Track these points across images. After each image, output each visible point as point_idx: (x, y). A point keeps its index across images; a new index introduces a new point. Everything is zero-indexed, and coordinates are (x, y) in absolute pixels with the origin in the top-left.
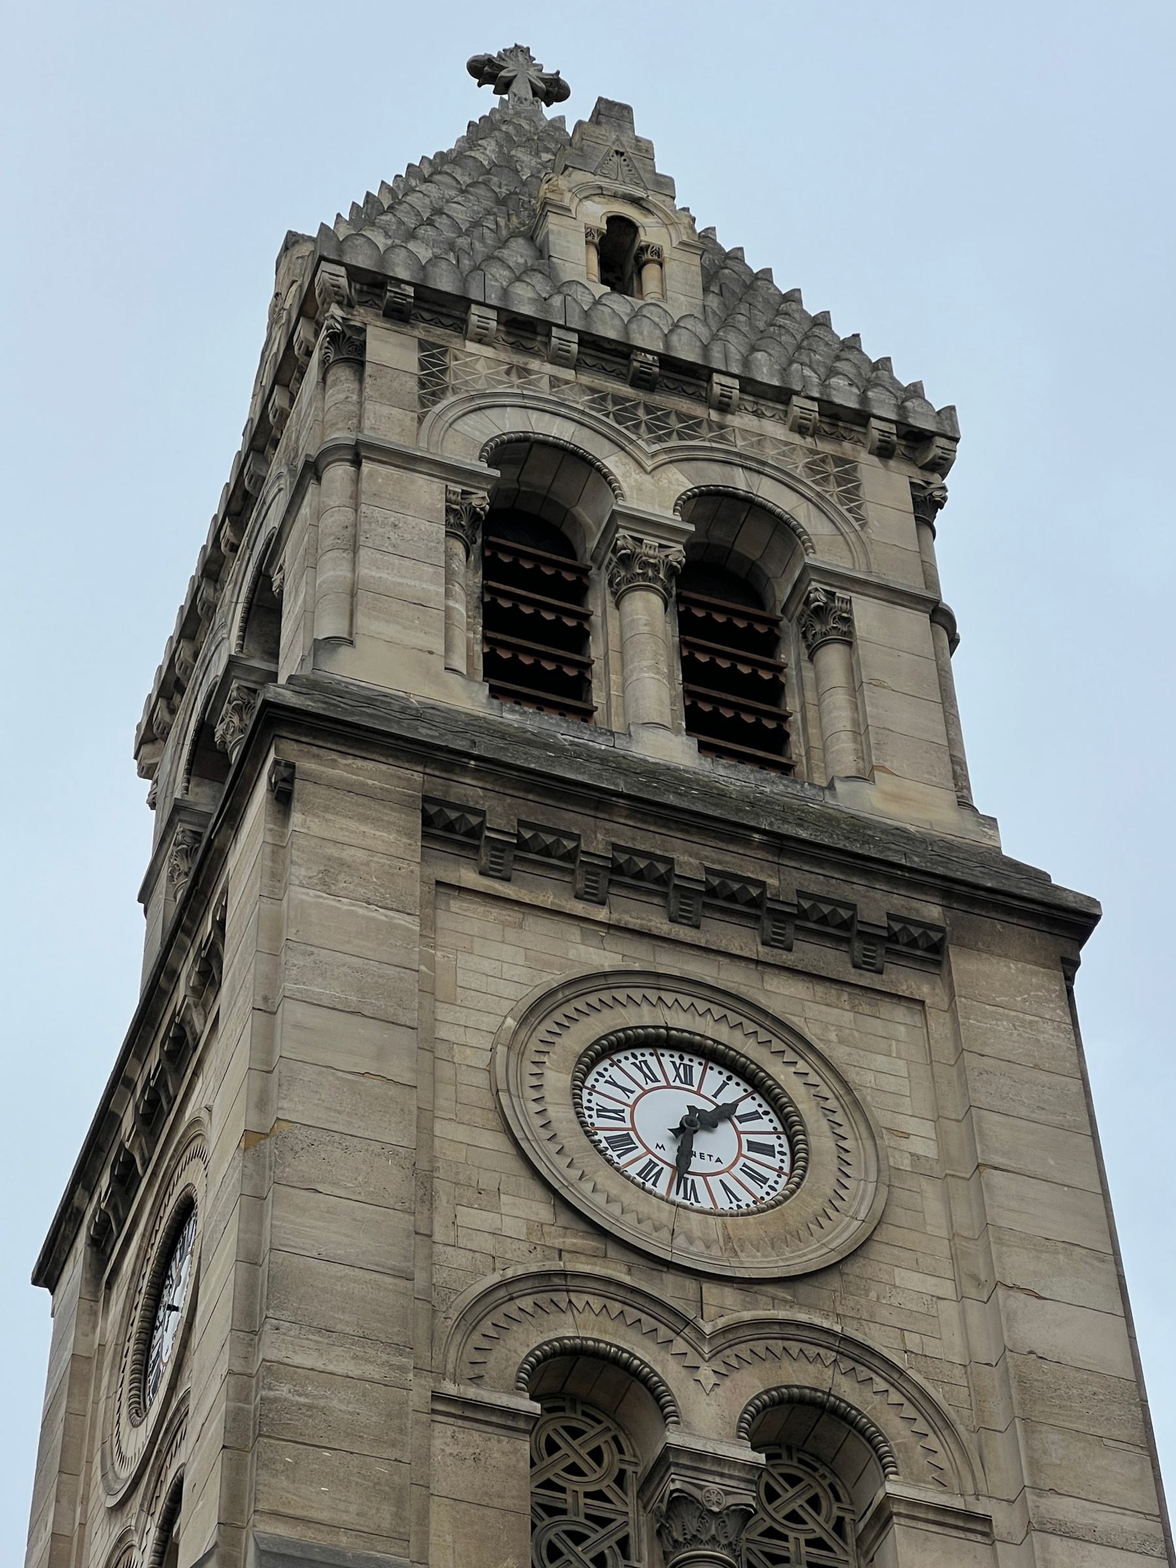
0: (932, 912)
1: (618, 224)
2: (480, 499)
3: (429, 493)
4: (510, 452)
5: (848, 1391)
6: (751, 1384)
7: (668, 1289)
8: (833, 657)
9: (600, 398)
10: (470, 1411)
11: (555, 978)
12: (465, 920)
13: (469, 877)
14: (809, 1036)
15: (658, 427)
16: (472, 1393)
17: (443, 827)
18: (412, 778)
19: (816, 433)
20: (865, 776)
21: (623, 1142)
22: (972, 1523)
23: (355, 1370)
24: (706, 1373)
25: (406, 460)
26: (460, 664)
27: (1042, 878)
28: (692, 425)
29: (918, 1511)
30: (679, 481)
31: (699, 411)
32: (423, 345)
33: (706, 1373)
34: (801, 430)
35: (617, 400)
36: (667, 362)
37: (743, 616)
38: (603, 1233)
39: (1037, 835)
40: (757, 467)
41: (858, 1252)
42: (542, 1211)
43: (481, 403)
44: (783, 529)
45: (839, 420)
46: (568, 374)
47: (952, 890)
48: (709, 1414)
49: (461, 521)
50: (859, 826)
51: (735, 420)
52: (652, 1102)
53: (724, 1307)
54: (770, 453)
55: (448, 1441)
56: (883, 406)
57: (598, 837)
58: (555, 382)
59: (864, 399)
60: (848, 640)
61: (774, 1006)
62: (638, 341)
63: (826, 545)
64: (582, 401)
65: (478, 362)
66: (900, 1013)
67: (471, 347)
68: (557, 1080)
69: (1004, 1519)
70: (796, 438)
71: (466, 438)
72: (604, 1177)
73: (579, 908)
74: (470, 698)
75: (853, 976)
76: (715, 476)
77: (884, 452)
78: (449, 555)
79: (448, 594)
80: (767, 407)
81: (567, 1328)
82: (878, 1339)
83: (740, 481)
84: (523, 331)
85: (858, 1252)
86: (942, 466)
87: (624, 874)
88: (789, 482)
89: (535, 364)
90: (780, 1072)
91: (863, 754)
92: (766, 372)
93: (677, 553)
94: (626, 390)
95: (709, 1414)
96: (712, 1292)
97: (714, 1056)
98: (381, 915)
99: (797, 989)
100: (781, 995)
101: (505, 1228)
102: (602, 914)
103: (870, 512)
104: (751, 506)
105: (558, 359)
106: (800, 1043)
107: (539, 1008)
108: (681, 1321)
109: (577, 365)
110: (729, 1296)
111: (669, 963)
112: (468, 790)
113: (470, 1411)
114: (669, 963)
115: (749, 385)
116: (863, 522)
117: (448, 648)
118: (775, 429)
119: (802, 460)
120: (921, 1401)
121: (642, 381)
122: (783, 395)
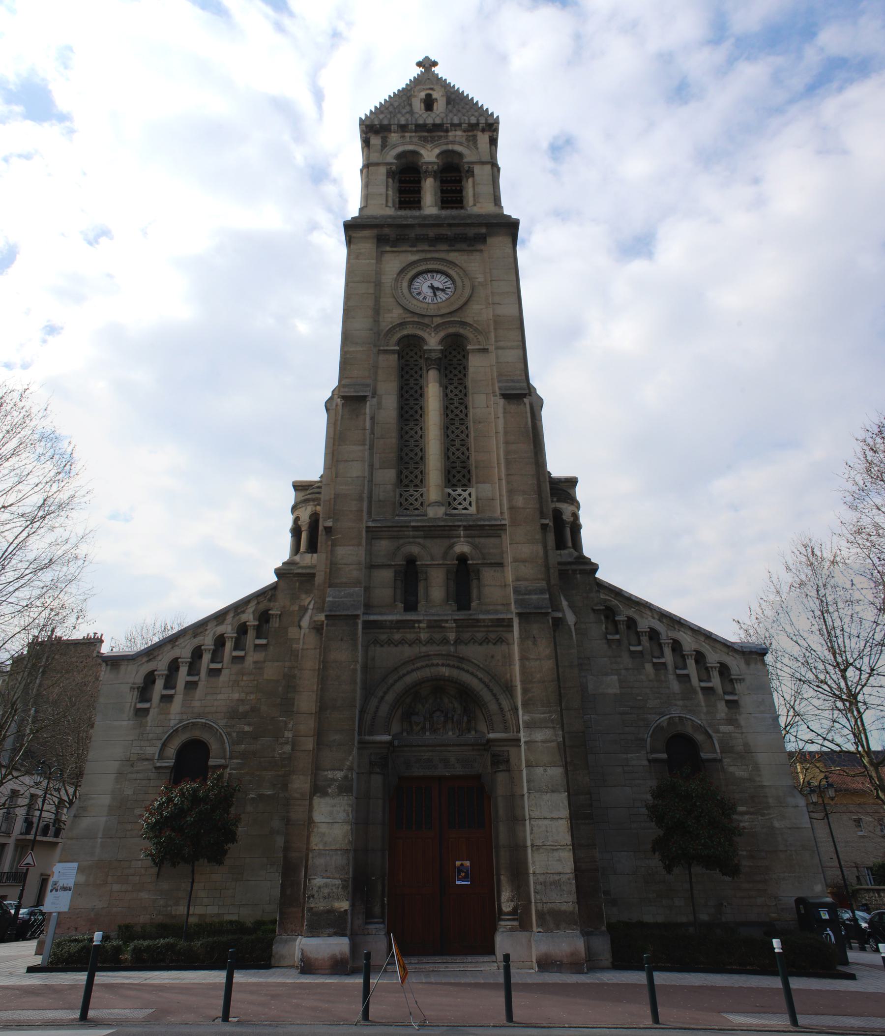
0: (483, 230)
1: (429, 96)
2: (394, 168)
3: (383, 170)
4: (399, 156)
5: (462, 331)
6: (442, 334)
7: (426, 321)
8: (470, 180)
9: (420, 137)
10: (386, 352)
11: (404, 265)
12: (387, 257)
13: (388, 249)
14: (457, 262)
15: (433, 140)
16: (386, 348)
17: (381, 240)
18: (375, 232)
19: (468, 131)
20: (475, 205)
21: (419, 294)
22: (485, 350)
23: (361, 349)
24: (433, 334)
25: (377, 164)
26: (390, 204)
27: (510, 217)
28: (440, 137)
29: (473, 351)
30: (437, 151)
31: (442, 134)
32: (382, 138)
33: (433, 334)
34: (464, 131)
35: (424, 137)
36: (434, 125)
37: (453, 177)
38: (412, 312)
39: (509, 208)
40: (453, 143)
41: (466, 303)
42: (401, 311)
43: (395, 146)
44: (460, 155)
45: (473, 127)
46: (413, 134)
47: (488, 225)
48: (433, 342)
49: (390, 174)
50: (479, 216)
51: (450, 134)
52: (424, 285)
53: (439, 320)
54: (457, 139)
55: (382, 358)
56: (482, 121)
57: (412, 234)
58: (410, 137)
59: (478, 120)
60: (473, 176)
61: (450, 259)
62: (428, 122)
63: (469, 155)
64: (415, 140)
65: (394, 137)
66: (478, 253)
67: (393, 135)
68: (405, 284)
69: (492, 348)
70: (464, 134)
71: (390, 156)
72: (415, 302)
73: (410, 249)
74: (390, 211)
75: (467, 248)
76: (444, 148)
77: (483, 131)
78: (387, 182)
79: (387, 190)
80: (458, 128)
81: (405, 332)
82: (469, 320)
83: (450, 147)
84: (403, 128)
85: (466, 303)
86: (496, 130)
87: (420, 239)
88: (461, 144)
89: (406, 134)
90: (451, 272)
91: (474, 200)
92: (456, 121)
93: (436, 167)
94: (426, 134)
95: (433, 342)
96: (435, 319)
97: (438, 272)
98: (368, 261)
99: (456, 254)
100: (453, 256)
101: (393, 316)
102: (415, 249)
103: (479, 146)
104: (453, 152)
105: (411, 132)
106: (455, 265)
107: (402, 271)
108: (427, 326)
109: (416, 131)
110: (438, 319)
111: (429, 256)
112: (386, 231)
113: (386, 352)
114: (429, 256)
115: (452, 125)
116: (477, 149)
117: (387, 201)
118: (459, 133)
119: (464, 139)
120: (476, 329)
121: (429, 131)
122: (460, 125)
